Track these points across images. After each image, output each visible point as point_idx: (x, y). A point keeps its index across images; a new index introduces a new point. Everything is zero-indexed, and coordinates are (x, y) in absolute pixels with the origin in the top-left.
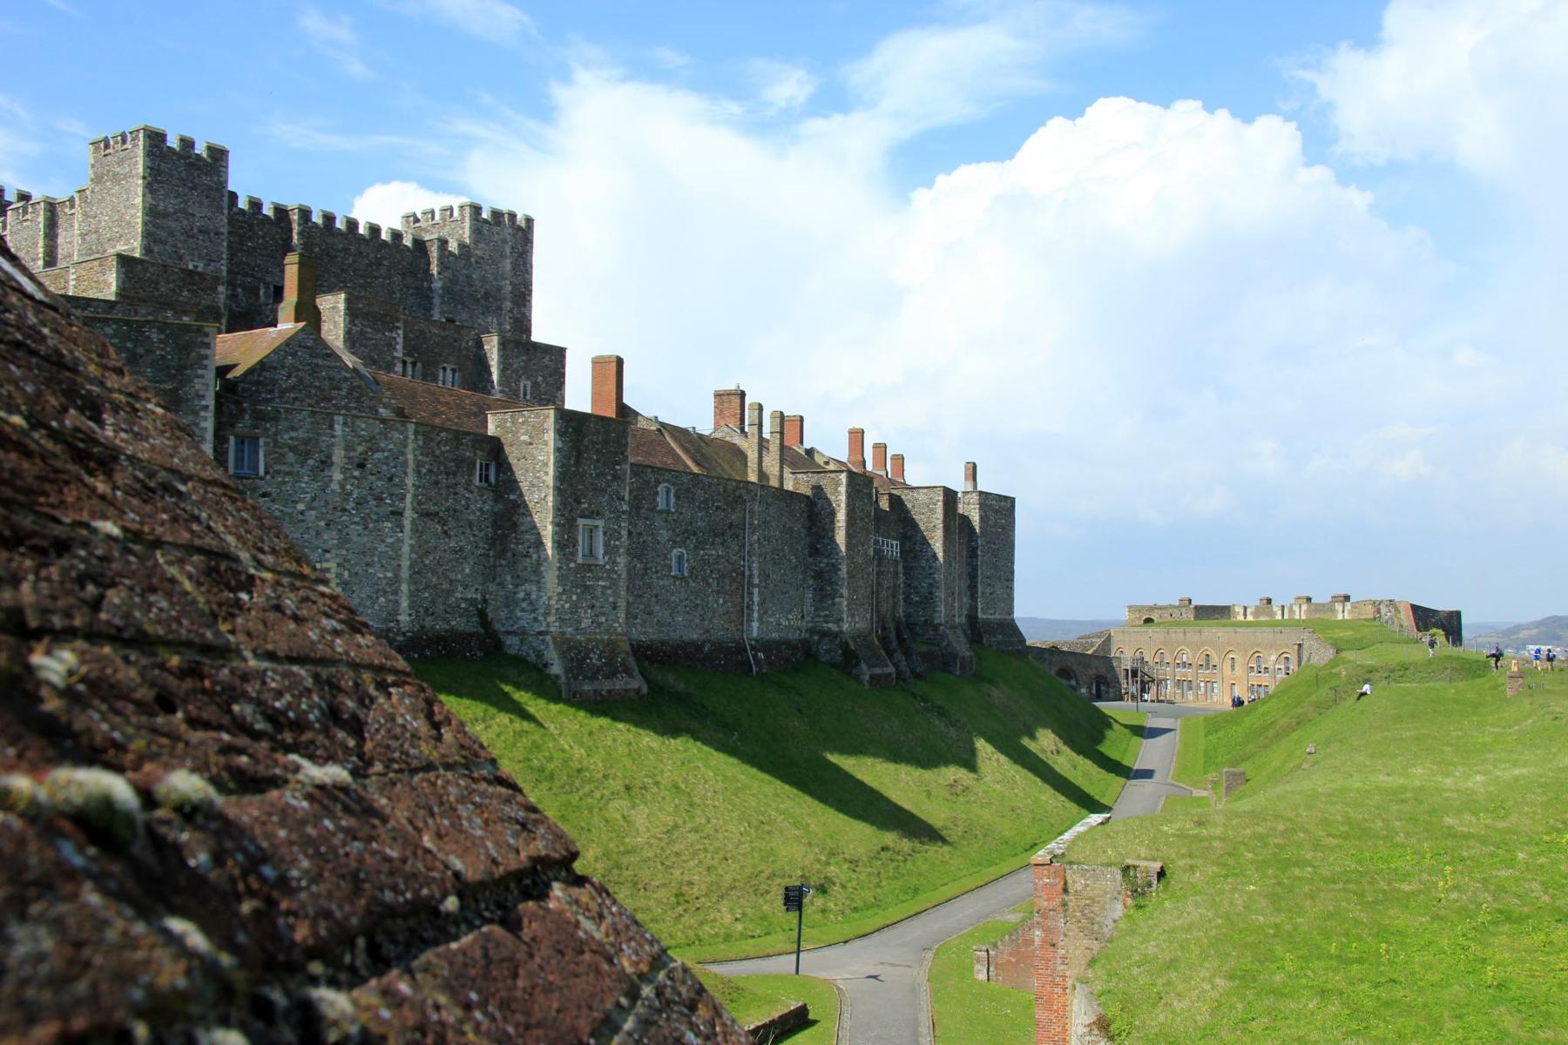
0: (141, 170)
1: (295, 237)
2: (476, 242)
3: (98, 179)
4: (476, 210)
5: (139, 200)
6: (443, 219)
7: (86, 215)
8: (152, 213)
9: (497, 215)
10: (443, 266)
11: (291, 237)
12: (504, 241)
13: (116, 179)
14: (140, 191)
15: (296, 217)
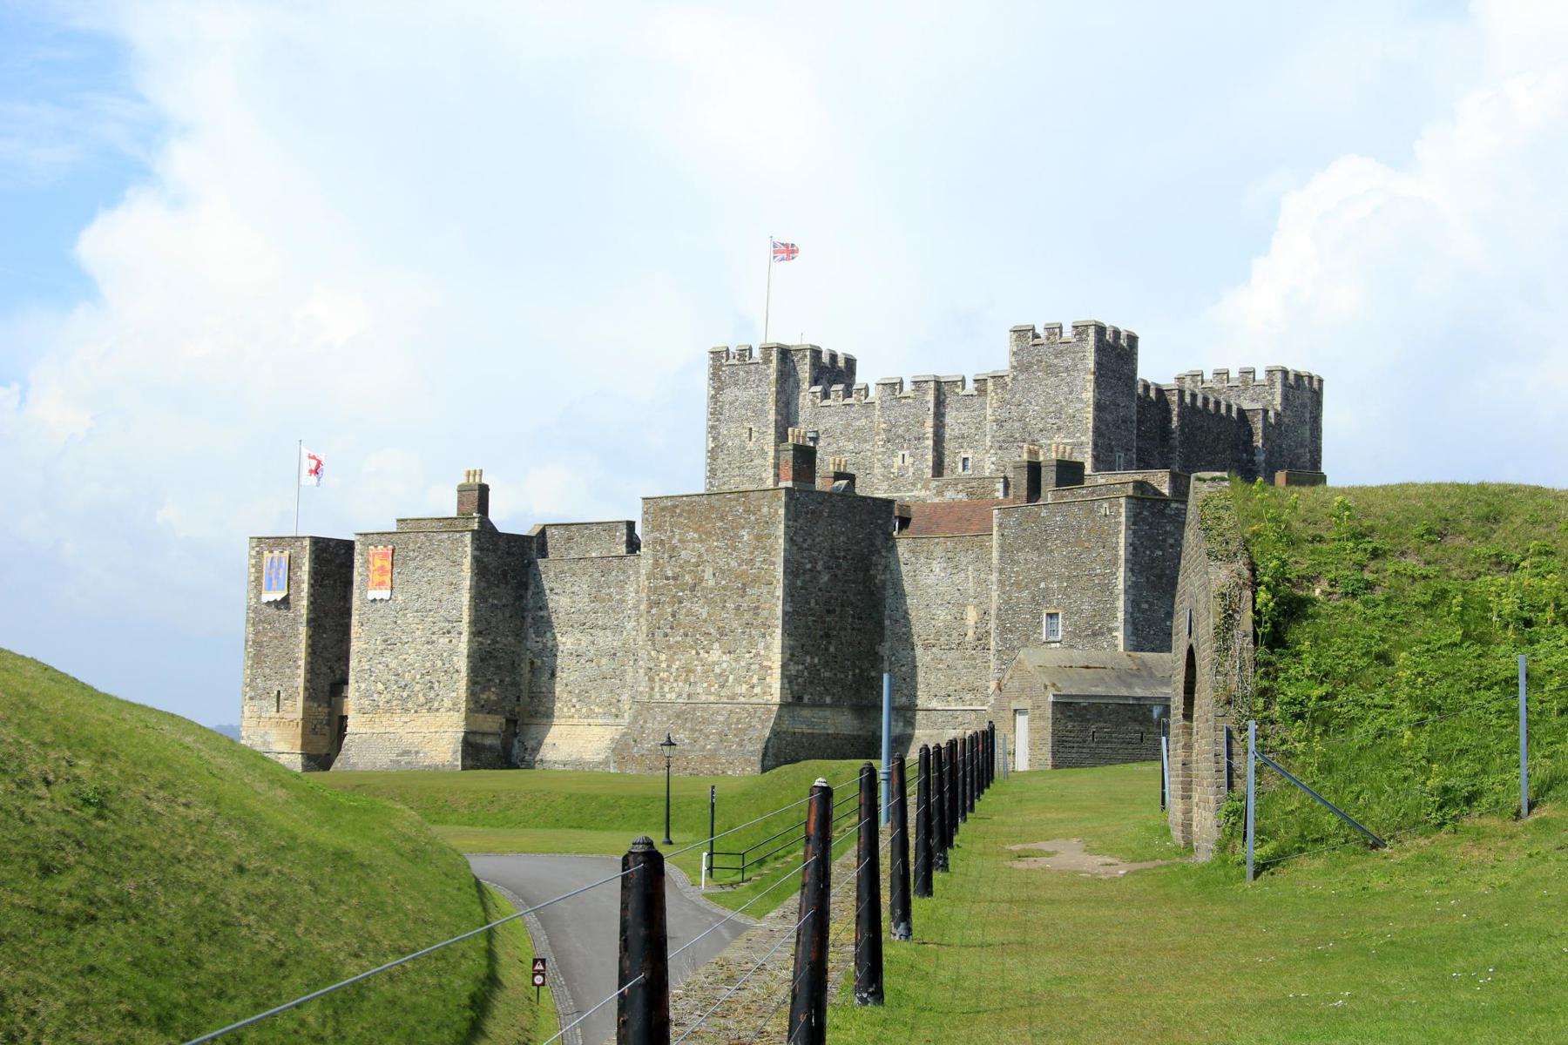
0: (1091, 365)
1: (1175, 419)
2: (1285, 409)
3: (1022, 367)
4: (1285, 373)
5: (1089, 395)
6: (1245, 382)
8: (1099, 407)
9: (1298, 377)
10: (1266, 437)
11: (1170, 421)
12: (1304, 406)
13: (1051, 371)
14: (1090, 386)
15: (1175, 398)
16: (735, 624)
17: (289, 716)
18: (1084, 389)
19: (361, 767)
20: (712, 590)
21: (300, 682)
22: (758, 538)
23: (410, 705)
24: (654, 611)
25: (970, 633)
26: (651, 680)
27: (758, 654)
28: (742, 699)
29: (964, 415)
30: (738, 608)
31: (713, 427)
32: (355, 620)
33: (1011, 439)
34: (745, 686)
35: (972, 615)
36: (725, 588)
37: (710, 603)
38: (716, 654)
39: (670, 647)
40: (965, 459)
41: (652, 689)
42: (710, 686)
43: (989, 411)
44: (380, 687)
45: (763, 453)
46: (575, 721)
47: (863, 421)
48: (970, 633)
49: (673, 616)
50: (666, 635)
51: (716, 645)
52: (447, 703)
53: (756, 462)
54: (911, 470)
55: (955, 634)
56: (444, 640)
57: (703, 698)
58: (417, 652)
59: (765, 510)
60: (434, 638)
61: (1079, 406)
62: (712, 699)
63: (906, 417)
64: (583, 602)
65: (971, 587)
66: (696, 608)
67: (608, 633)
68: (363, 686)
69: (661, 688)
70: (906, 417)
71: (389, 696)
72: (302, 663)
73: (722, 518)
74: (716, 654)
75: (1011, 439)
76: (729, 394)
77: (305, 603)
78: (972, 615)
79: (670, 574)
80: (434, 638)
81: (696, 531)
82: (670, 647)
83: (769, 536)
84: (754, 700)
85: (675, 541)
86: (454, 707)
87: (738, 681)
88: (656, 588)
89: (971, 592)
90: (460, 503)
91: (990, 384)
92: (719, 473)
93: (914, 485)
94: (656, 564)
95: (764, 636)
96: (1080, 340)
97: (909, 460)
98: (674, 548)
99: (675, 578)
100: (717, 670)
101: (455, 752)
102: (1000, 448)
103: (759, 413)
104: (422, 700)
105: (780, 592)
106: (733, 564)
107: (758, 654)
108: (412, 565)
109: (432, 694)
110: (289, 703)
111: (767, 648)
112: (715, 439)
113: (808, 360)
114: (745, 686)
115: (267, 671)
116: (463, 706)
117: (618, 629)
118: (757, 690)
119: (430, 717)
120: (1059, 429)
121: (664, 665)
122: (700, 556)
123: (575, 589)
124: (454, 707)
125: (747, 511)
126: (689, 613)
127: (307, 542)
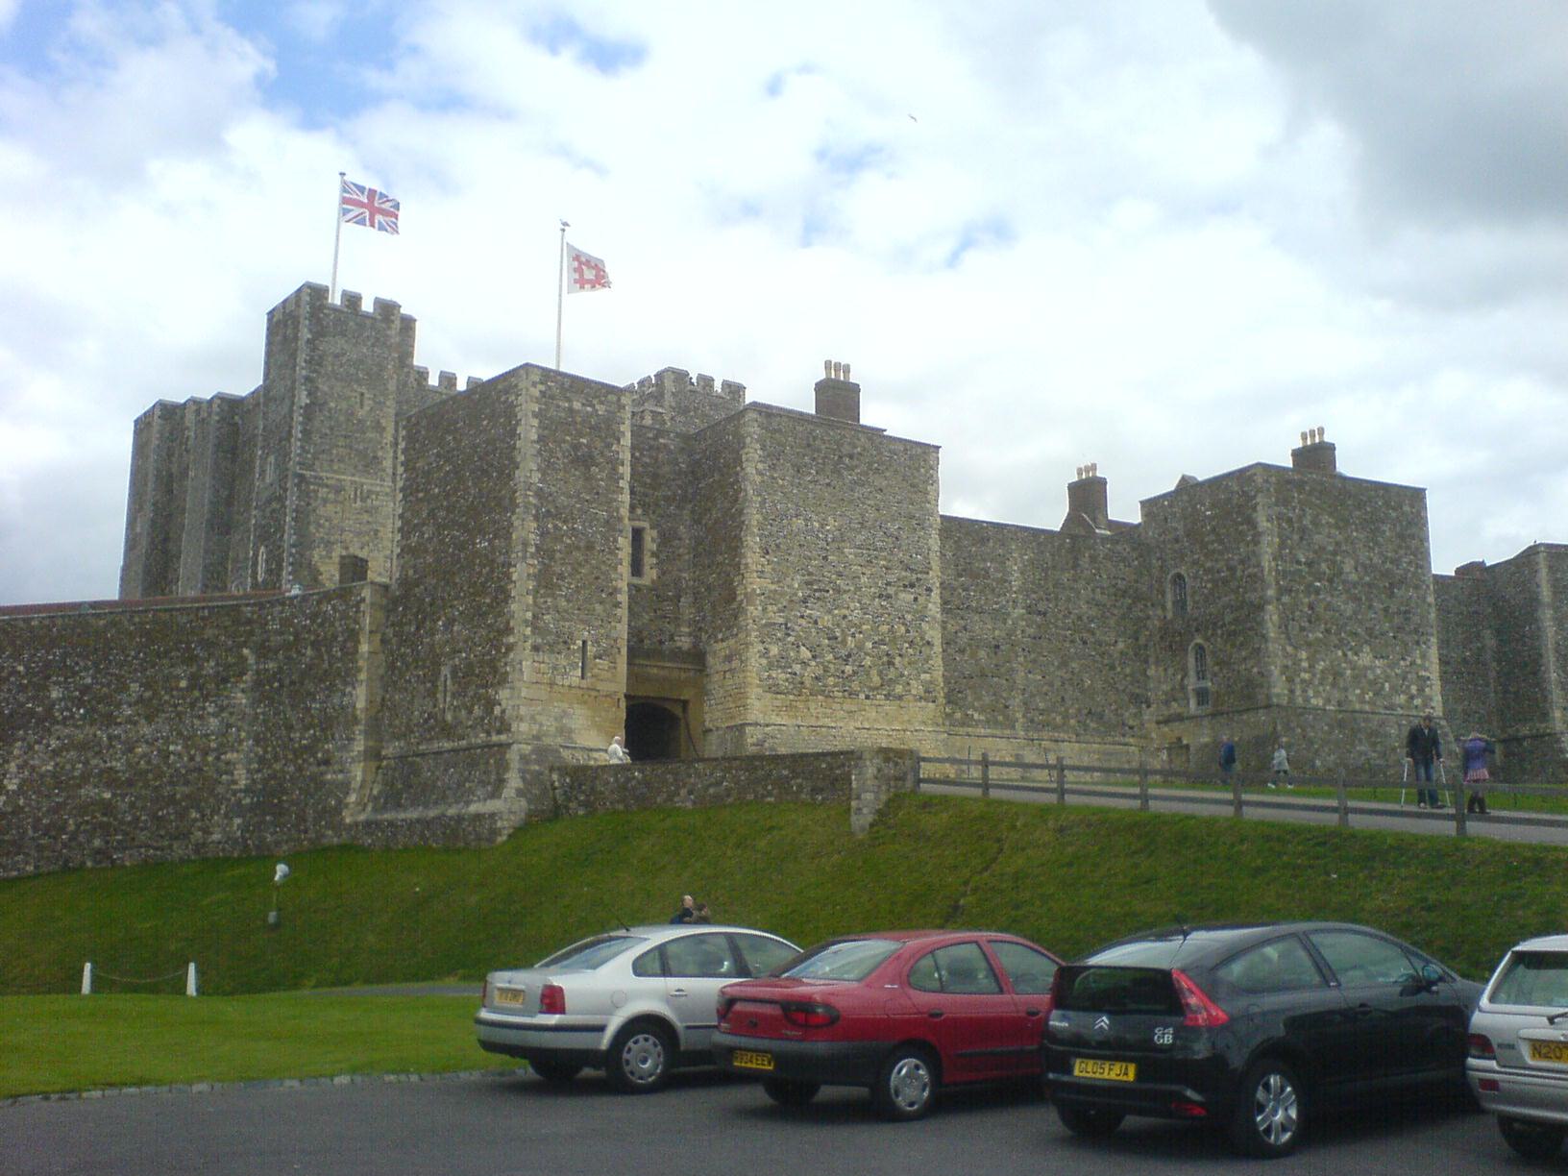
20: (1355, 585)
21: (622, 630)
22: (1401, 536)
24: (1286, 599)
26: (1290, 680)
27: (1413, 663)
30: (1386, 610)
31: (307, 379)
32: (752, 541)
34: (1402, 699)
36: (1369, 585)
37: (1356, 599)
38: (1365, 658)
39: (1309, 645)
41: (1292, 691)
42: (1363, 693)
44: (805, 653)
45: (379, 428)
49: (1311, 607)
50: (1302, 629)
51: (1366, 649)
52: (917, 688)
53: (370, 435)
56: (907, 597)
57: (1357, 707)
60: (891, 590)
62: (1367, 708)
66: (1339, 602)
68: (774, 650)
69: (1304, 691)
73: (1359, 508)
74: (1365, 658)
76: (332, 345)
81: (1331, 514)
82: (1309, 645)
86: (928, 695)
92: (316, 438)
94: (1282, 545)
95: (1418, 643)
98: (1303, 530)
99: (1309, 564)
100: (1371, 677)
104: (876, 680)
107: (1413, 663)
109: (892, 674)
110: (603, 663)
111: (1424, 657)
112: (309, 394)
114: (1402, 699)
117: (1000, 616)
118: (1418, 702)
119: (890, 707)
121: (1305, 664)
122: (1338, 544)
124: (928, 695)
126: (1329, 607)
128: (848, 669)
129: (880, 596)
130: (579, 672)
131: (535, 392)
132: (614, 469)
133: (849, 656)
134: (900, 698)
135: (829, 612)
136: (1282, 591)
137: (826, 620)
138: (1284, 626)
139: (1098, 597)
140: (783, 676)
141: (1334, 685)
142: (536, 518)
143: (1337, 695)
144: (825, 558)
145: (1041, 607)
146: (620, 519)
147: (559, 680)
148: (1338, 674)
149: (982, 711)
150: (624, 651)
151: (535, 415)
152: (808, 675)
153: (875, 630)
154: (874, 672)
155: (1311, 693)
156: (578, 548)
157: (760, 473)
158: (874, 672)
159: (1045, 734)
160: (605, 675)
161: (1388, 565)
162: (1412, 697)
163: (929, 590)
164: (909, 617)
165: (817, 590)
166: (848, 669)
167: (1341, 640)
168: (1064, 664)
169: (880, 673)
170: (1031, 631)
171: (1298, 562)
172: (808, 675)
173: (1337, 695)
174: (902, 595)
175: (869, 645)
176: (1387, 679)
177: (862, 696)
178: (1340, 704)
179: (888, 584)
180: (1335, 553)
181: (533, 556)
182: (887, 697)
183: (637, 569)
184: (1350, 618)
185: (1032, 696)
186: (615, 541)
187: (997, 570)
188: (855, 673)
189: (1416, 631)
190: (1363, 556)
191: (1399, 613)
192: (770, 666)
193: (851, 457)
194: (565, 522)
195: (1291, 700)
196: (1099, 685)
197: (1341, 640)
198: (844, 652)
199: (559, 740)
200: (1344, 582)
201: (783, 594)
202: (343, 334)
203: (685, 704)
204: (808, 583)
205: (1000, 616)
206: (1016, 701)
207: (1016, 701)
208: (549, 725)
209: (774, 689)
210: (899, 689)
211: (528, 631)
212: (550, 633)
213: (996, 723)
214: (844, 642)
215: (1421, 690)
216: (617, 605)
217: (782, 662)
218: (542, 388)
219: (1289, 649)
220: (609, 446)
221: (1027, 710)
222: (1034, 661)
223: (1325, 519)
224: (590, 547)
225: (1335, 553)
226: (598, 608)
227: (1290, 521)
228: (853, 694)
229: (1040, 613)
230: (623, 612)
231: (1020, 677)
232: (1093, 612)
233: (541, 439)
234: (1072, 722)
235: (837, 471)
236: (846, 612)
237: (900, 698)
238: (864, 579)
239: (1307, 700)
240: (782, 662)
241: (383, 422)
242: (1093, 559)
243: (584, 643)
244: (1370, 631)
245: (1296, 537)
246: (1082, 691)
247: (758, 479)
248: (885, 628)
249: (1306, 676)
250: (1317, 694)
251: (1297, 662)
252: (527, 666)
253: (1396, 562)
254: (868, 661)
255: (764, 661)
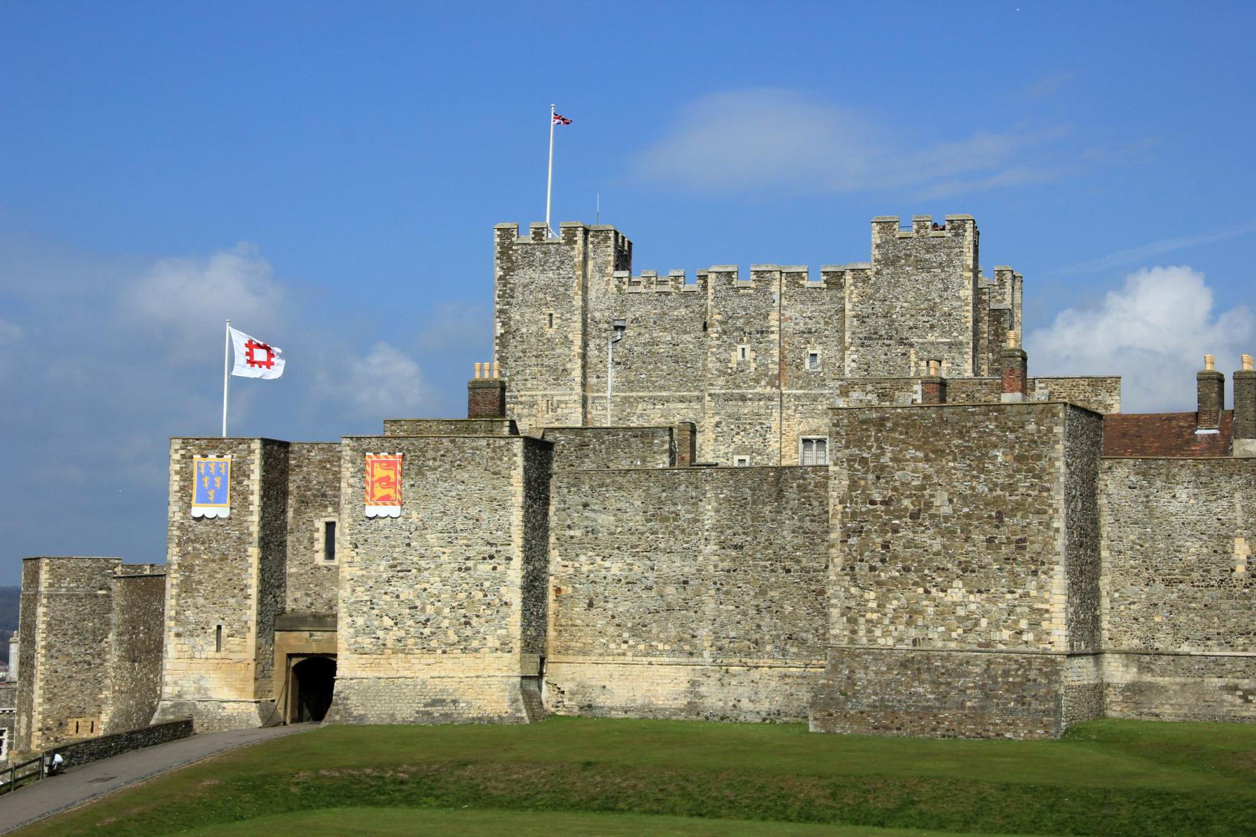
3: (889, 261)
7: (864, 298)
13: (923, 266)
16: (988, 559)
17: (236, 657)
18: (962, 286)
19: (372, 720)
20: (946, 518)
22: (1020, 459)
23: (434, 644)
24: (854, 540)
25: (1240, 569)
28: (1001, 647)
29: (810, 309)
30: (990, 541)
31: (501, 311)
33: (874, 336)
34: (1006, 634)
35: (1241, 549)
36: (968, 516)
38: (957, 592)
39: (880, 584)
40: (814, 355)
41: (854, 632)
42: (950, 630)
43: (848, 306)
44: (388, 622)
45: (567, 342)
46: (629, 658)
47: (683, 311)
48: (1240, 569)
50: (872, 569)
51: (958, 583)
52: (492, 642)
54: (753, 365)
55: (1215, 571)
56: (485, 567)
57: (940, 644)
58: (444, 582)
59: (1032, 427)
60: (470, 564)
61: (956, 304)
62: (953, 645)
63: (745, 309)
64: (637, 521)
65: (1239, 516)
66: (923, 538)
67: (678, 559)
68: (360, 621)
69: (869, 631)
70: (745, 309)
71: (402, 633)
72: (253, 591)
73: (961, 435)
74: (957, 592)
75: (874, 336)
76: (521, 277)
77: (255, 518)
78: (1241, 549)
79: (878, 498)
80: (470, 564)
81: (917, 448)
82: (880, 584)
83: (1039, 457)
84: (1023, 648)
85: (885, 459)
86: (505, 647)
87: (996, 625)
88: (854, 515)
89: (1240, 522)
90: (473, 402)
91: (849, 278)
92: (511, 362)
93: (757, 381)
94: (853, 485)
95: (1035, 573)
96: (957, 235)
97: (750, 355)
98: (883, 468)
100: (961, 612)
101: (515, 701)
102: (862, 345)
103: (561, 298)
104: (453, 637)
105: (1059, 523)
106: (982, 488)
107: (1027, 595)
108: (431, 476)
109: (468, 631)
110: (236, 640)
111: (1041, 588)
112: (504, 324)
113: (611, 242)
114: (1006, 634)
115: (201, 601)
116: (517, 645)
117: (691, 553)
118: (1028, 637)
119: (468, 660)
120: (932, 327)
121: (873, 605)
123: (623, 505)
124: (505, 647)
125: (1004, 428)
127: (256, 446)
128: (427, 631)
129: (460, 569)
130: (214, 648)
131: (177, 457)
132: (245, 498)
133: (428, 620)
134: (476, 650)
135: (411, 586)
136: (847, 534)
137: (406, 593)
138: (850, 569)
139: (807, 524)
140: (369, 641)
141: (909, 624)
142: (179, 545)
143: (913, 633)
144: (408, 545)
145: (737, 540)
146: (250, 535)
147: (197, 655)
148: (913, 613)
149: (667, 641)
150: (254, 629)
151: (177, 473)
152: (390, 639)
153: (454, 595)
154: (451, 632)
155: (878, 632)
156: (214, 561)
157: (351, 486)
158: (451, 632)
159: (735, 660)
160: (239, 648)
161: (999, 492)
162: (1020, 633)
163: (509, 559)
164: (487, 584)
165: (399, 570)
166: (427, 631)
167: (923, 578)
168: (762, 592)
169: (457, 633)
170: (726, 565)
171: (873, 503)
172: (390, 639)
173: (913, 633)
174: (480, 567)
175: (447, 610)
176: (985, 613)
177: (439, 651)
178: (915, 642)
179: (468, 559)
180: (923, 488)
181: (176, 571)
182: (464, 650)
183: (330, 554)
184: (937, 554)
185: (723, 625)
186: (246, 551)
187: (688, 512)
188: (433, 633)
189: (1033, 560)
190: (961, 488)
191: (1009, 542)
192: (357, 634)
193: (435, 459)
194: (203, 543)
195: (852, 641)
196: (802, 611)
197: (923, 578)
198: (423, 618)
199: (197, 697)
200: (932, 516)
201: (368, 578)
202: (531, 265)
203: (335, 655)
204: (391, 567)
205: (691, 553)
206: (704, 632)
207: (704, 632)
208: (189, 687)
209: (359, 651)
210: (475, 644)
211: (172, 623)
212: (190, 623)
213: (682, 651)
214: (423, 610)
215: (1034, 625)
216: (247, 597)
217: (367, 630)
218: (183, 452)
219: (853, 590)
220: (240, 483)
221: (718, 638)
222: (727, 593)
223: (912, 452)
224: (224, 558)
225: (923, 488)
226: (232, 601)
227: (864, 461)
228: (431, 651)
229: (735, 547)
230: (253, 602)
231: (710, 607)
232: (799, 541)
233: (182, 489)
234: (769, 648)
235: (420, 473)
236: (427, 586)
237: (476, 650)
238: (444, 558)
239: (873, 640)
240: (367, 630)
241: (570, 336)
242: (802, 488)
243: (219, 627)
244: (965, 568)
245: (871, 477)
246: (783, 618)
247: (350, 490)
248: (463, 596)
249: (875, 616)
250: (886, 633)
251: (862, 603)
252: (172, 647)
253: (1011, 488)
254: (446, 623)
255: (352, 630)
